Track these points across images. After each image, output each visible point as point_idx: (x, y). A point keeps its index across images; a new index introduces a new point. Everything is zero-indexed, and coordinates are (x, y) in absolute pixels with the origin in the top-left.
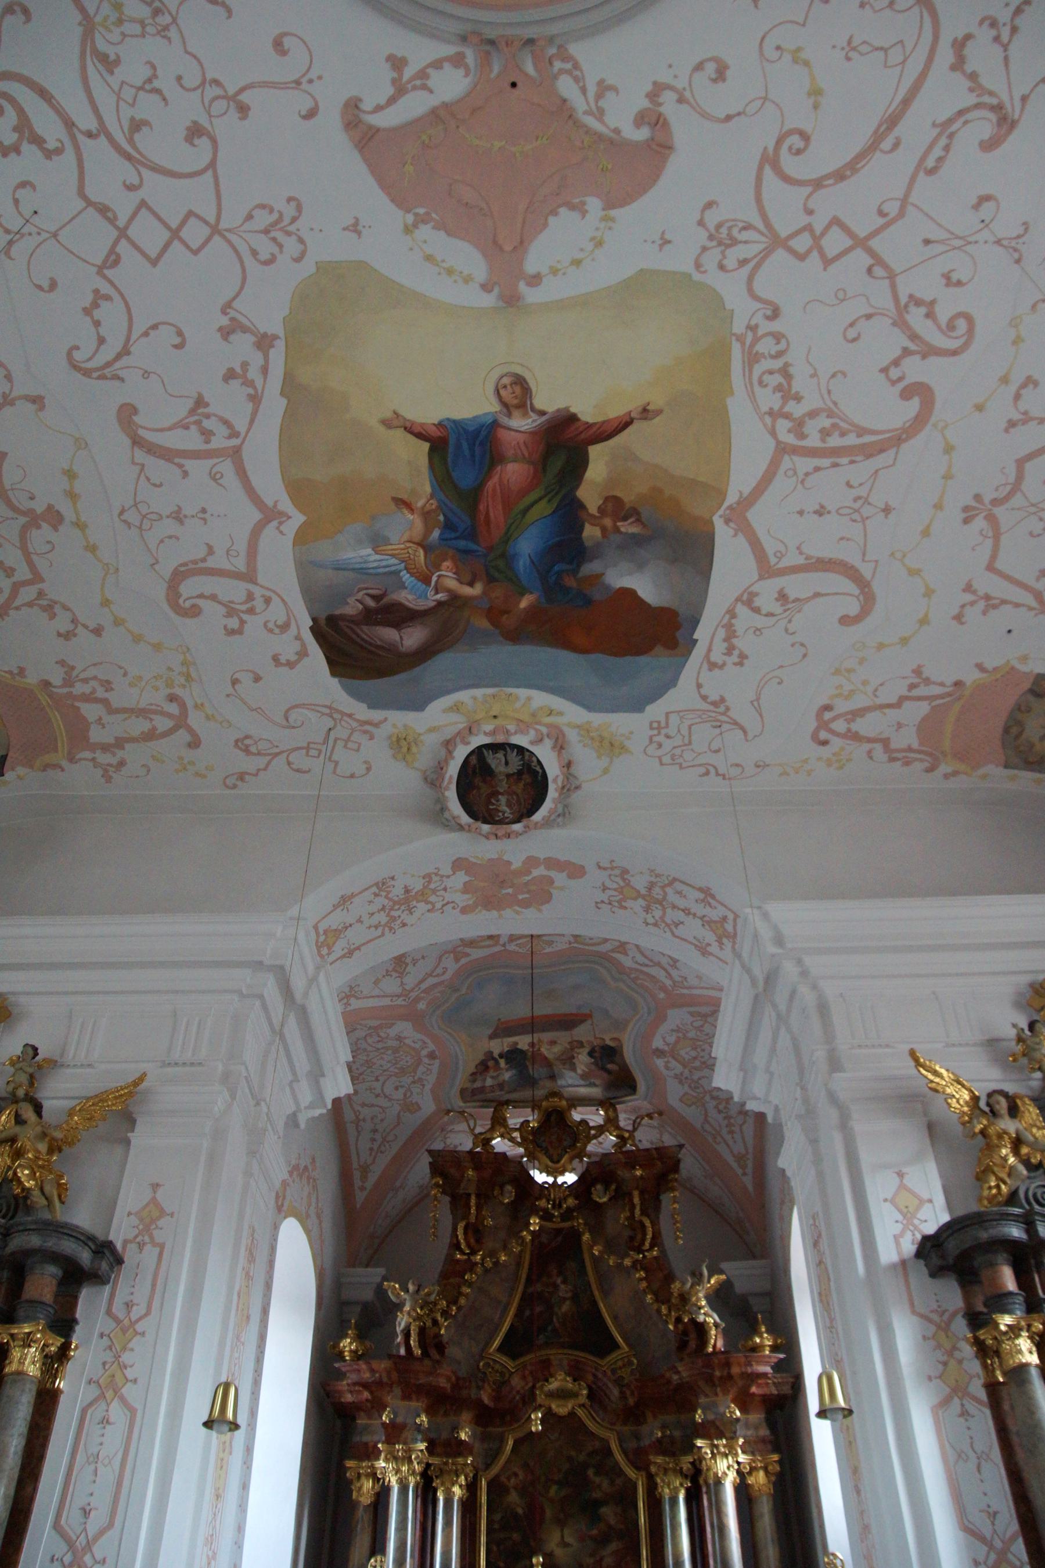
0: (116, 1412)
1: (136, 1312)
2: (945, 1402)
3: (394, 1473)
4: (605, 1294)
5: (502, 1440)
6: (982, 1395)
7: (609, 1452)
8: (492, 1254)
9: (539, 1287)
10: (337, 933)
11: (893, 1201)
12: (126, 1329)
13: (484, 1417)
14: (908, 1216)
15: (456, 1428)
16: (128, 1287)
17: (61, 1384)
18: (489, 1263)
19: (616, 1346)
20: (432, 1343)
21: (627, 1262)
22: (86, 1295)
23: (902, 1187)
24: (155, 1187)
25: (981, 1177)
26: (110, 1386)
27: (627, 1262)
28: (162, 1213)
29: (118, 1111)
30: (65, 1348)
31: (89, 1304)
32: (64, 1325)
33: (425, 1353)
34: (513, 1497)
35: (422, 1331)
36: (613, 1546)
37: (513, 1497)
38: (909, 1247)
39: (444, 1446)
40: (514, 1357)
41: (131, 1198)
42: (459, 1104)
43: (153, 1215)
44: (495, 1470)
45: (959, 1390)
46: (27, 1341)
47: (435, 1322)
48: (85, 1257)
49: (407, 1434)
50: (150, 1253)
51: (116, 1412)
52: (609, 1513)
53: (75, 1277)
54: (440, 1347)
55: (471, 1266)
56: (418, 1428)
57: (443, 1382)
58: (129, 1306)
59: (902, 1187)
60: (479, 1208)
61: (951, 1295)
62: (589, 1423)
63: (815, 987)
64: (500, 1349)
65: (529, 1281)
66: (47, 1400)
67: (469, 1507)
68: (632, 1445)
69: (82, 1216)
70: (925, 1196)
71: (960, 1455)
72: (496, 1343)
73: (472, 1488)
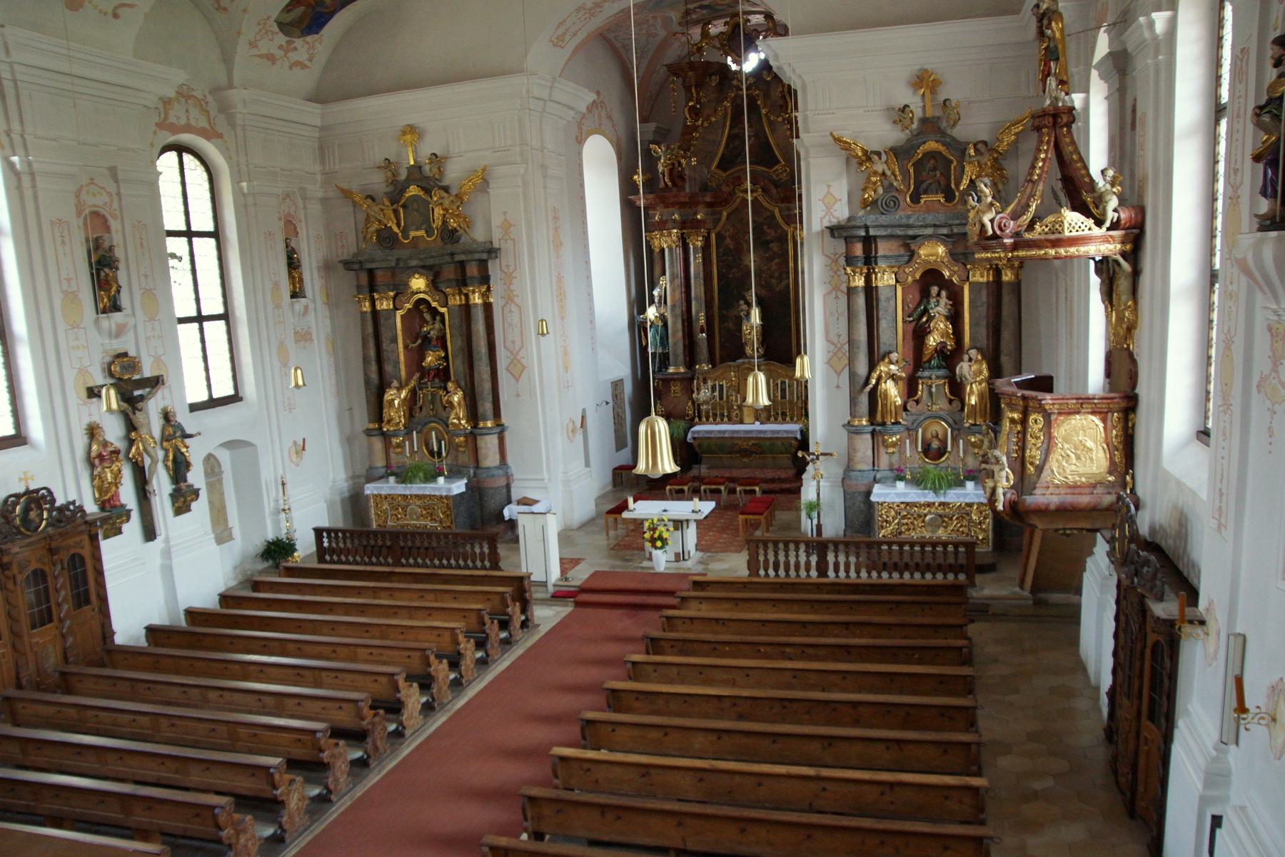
0: (514, 308)
1: (511, 268)
2: (830, 293)
3: (666, 241)
4: (772, 131)
5: (720, 213)
6: (845, 290)
7: (773, 217)
8: (708, 117)
9: (736, 131)
10: (564, 34)
11: (822, 201)
12: (509, 278)
13: (709, 205)
14: (829, 208)
15: (696, 214)
16: (506, 259)
17: (492, 300)
18: (706, 124)
19: (778, 162)
20: (677, 176)
21: (780, 119)
22: (490, 264)
23: (829, 193)
24: (505, 213)
25: (865, 190)
26: (509, 298)
27: (780, 119)
28: (511, 225)
29: (483, 181)
30: (489, 289)
31: (493, 268)
32: (485, 279)
33: (674, 184)
34: (728, 241)
35: (671, 171)
36: (777, 261)
37: (728, 241)
38: (826, 224)
39: (688, 226)
40: (725, 171)
41: (496, 220)
42: (679, 29)
43: (507, 226)
44: (718, 229)
45: (836, 288)
46: (474, 292)
47: (680, 164)
48: (484, 256)
49: (669, 225)
50: (510, 243)
51: (514, 308)
52: (774, 247)
53: (483, 264)
54: (682, 178)
55: (695, 128)
56: (674, 221)
57: (683, 200)
58: (508, 266)
59: (829, 193)
60: (698, 94)
61: (841, 247)
62: (765, 204)
63: (800, 77)
64: (718, 167)
65: (731, 127)
66: (488, 307)
67: (706, 249)
68: (786, 213)
69: (479, 234)
70: (838, 197)
71: (831, 314)
72: (715, 164)
73: (707, 240)
